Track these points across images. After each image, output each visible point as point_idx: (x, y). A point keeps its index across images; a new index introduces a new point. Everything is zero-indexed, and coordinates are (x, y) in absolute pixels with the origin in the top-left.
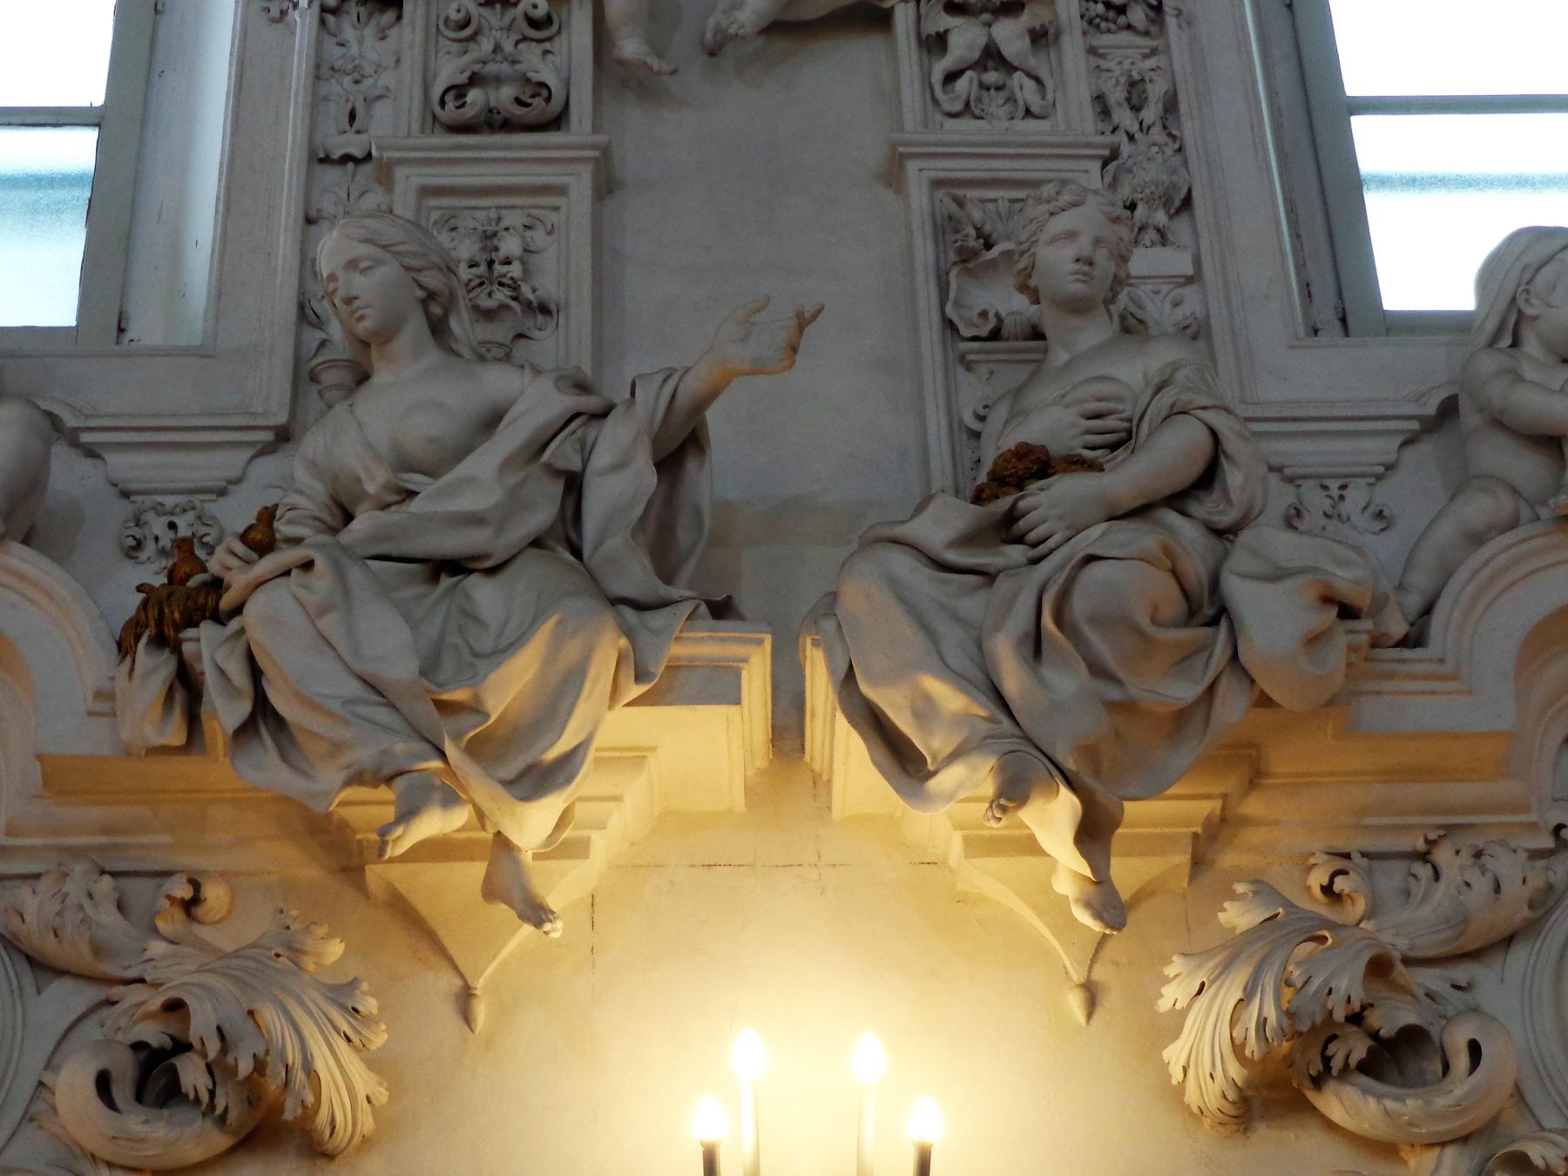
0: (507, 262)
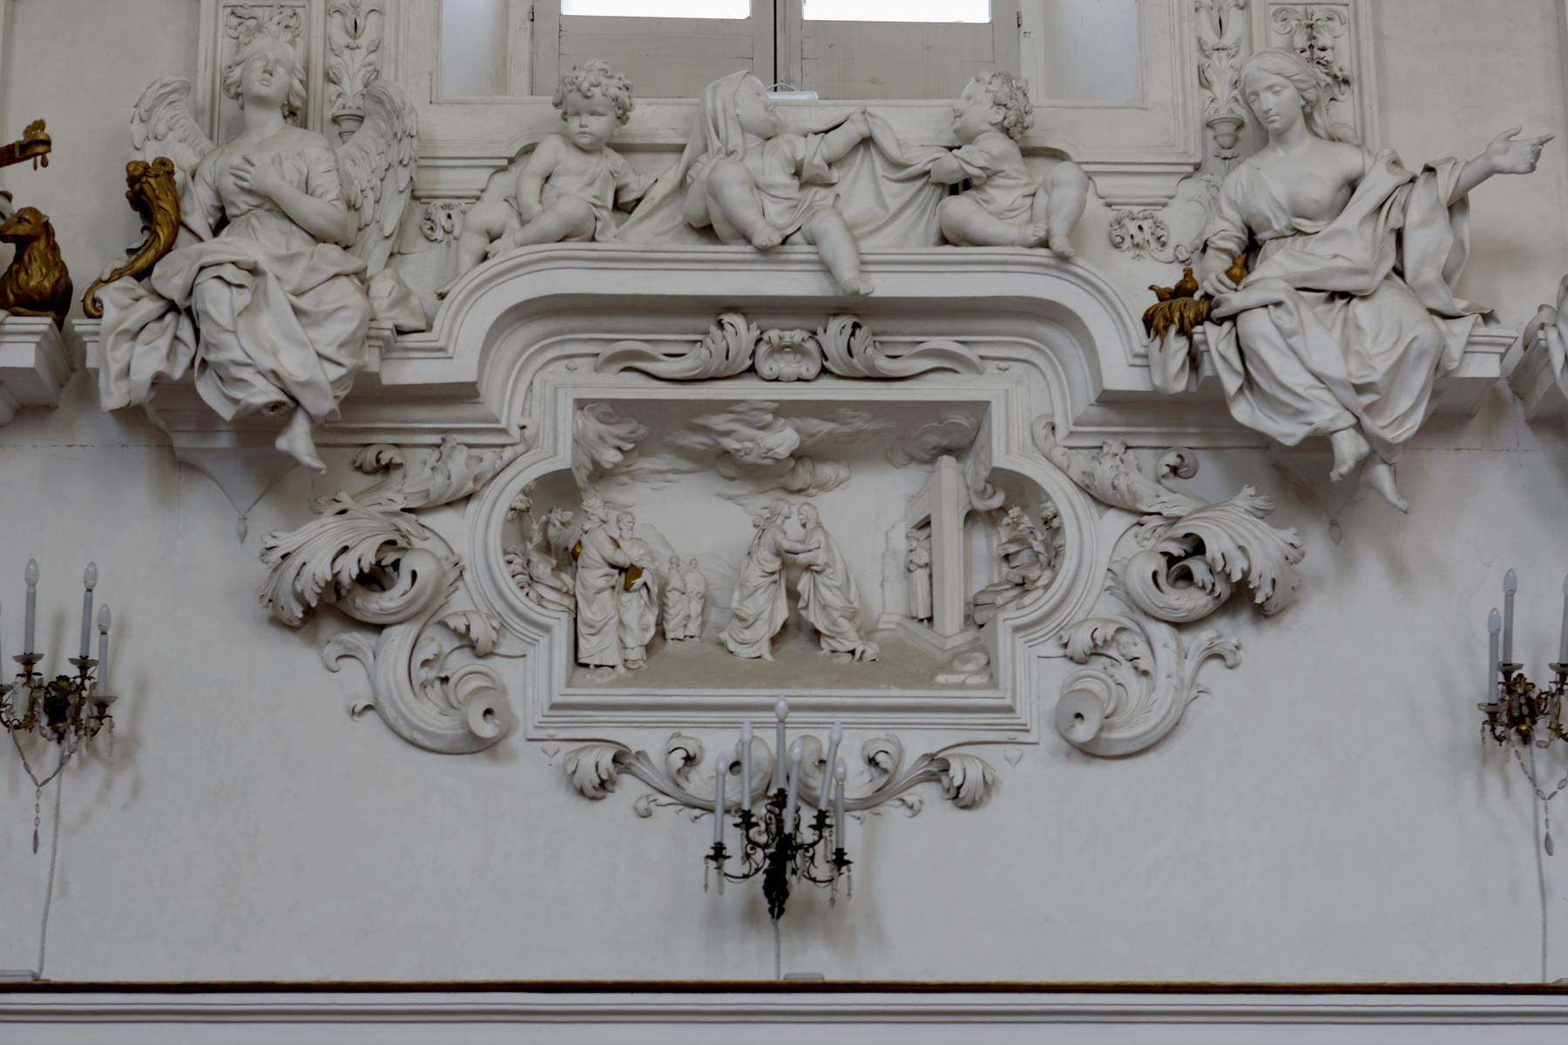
0: (1323, 49)
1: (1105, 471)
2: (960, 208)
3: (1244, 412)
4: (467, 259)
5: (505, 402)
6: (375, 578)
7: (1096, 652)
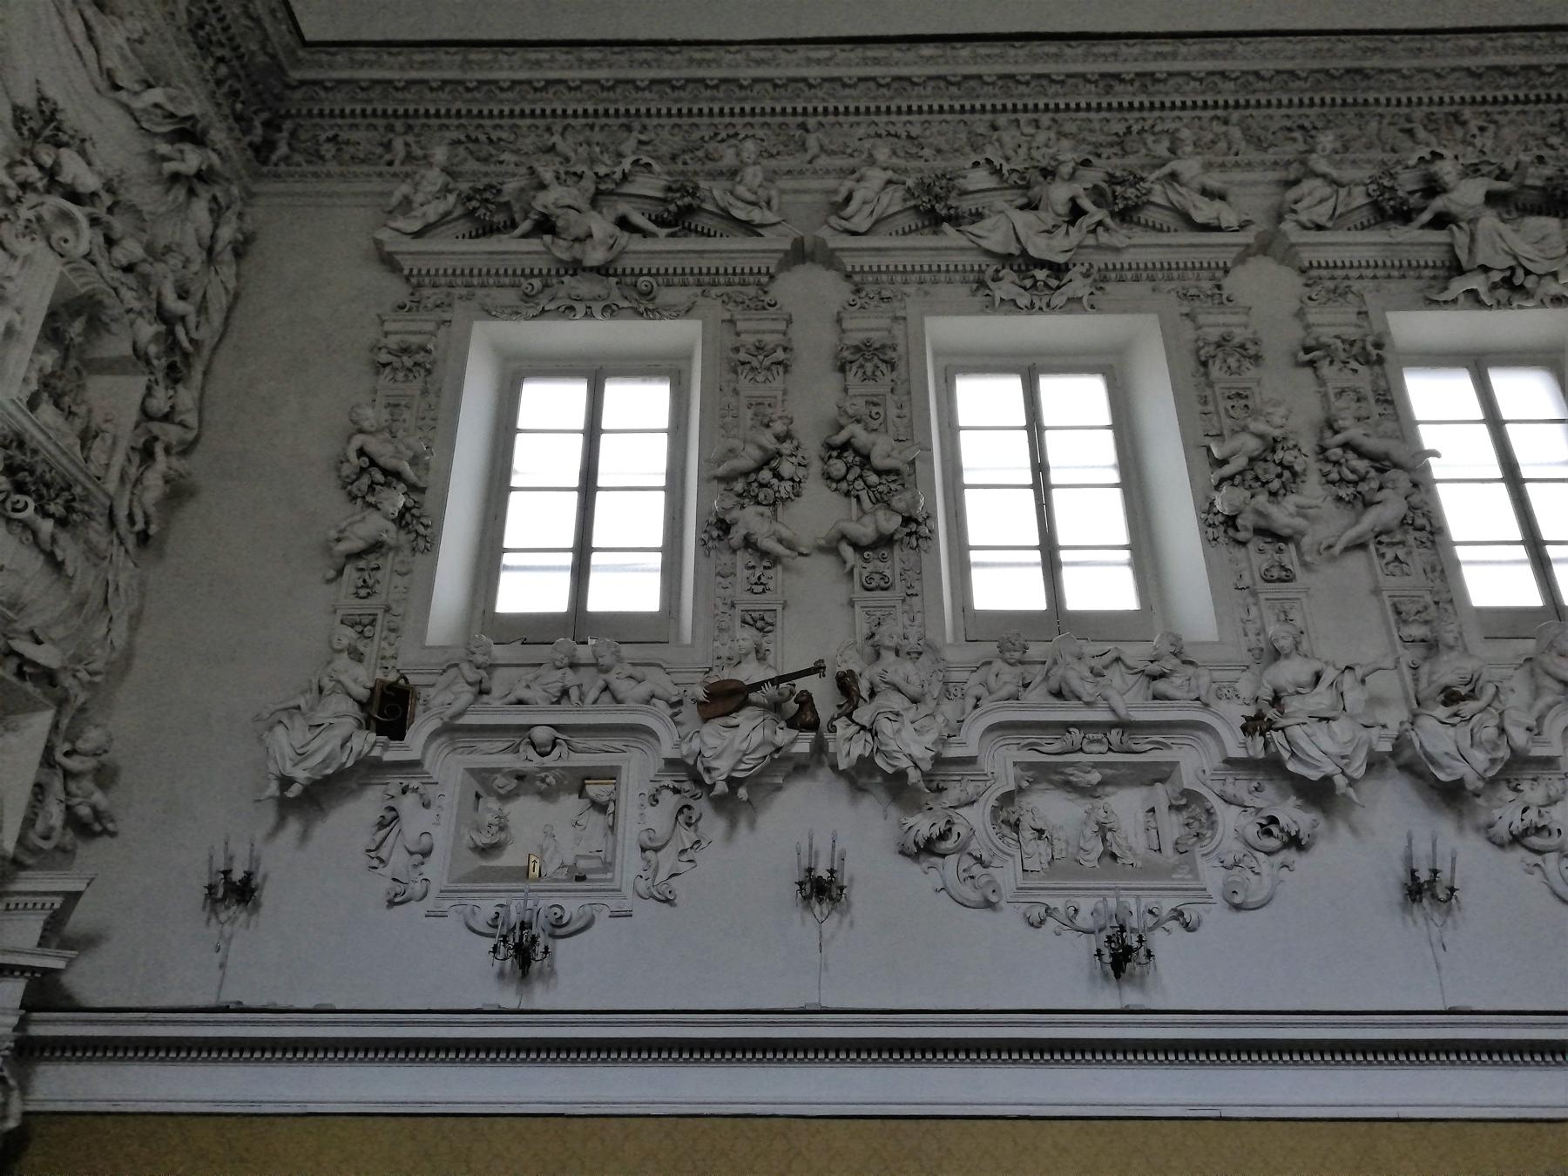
1: (1230, 790)
2: (1161, 686)
3: (1292, 766)
4: (969, 708)
5: (986, 765)
6: (943, 836)
7: (1236, 864)
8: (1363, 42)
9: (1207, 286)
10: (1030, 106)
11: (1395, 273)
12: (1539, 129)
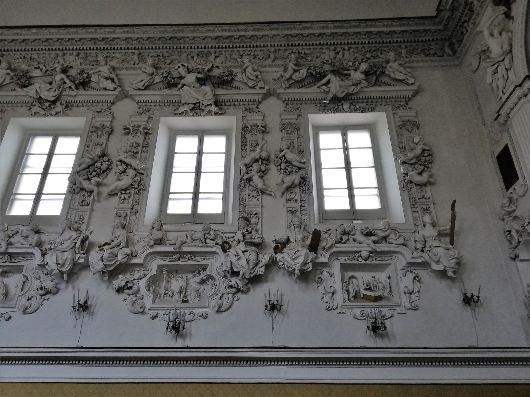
8: (176, 28)
9: (105, 108)
10: (71, 49)
11: (166, 104)
12: (236, 57)
